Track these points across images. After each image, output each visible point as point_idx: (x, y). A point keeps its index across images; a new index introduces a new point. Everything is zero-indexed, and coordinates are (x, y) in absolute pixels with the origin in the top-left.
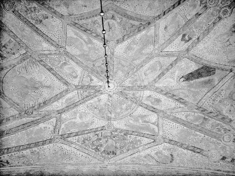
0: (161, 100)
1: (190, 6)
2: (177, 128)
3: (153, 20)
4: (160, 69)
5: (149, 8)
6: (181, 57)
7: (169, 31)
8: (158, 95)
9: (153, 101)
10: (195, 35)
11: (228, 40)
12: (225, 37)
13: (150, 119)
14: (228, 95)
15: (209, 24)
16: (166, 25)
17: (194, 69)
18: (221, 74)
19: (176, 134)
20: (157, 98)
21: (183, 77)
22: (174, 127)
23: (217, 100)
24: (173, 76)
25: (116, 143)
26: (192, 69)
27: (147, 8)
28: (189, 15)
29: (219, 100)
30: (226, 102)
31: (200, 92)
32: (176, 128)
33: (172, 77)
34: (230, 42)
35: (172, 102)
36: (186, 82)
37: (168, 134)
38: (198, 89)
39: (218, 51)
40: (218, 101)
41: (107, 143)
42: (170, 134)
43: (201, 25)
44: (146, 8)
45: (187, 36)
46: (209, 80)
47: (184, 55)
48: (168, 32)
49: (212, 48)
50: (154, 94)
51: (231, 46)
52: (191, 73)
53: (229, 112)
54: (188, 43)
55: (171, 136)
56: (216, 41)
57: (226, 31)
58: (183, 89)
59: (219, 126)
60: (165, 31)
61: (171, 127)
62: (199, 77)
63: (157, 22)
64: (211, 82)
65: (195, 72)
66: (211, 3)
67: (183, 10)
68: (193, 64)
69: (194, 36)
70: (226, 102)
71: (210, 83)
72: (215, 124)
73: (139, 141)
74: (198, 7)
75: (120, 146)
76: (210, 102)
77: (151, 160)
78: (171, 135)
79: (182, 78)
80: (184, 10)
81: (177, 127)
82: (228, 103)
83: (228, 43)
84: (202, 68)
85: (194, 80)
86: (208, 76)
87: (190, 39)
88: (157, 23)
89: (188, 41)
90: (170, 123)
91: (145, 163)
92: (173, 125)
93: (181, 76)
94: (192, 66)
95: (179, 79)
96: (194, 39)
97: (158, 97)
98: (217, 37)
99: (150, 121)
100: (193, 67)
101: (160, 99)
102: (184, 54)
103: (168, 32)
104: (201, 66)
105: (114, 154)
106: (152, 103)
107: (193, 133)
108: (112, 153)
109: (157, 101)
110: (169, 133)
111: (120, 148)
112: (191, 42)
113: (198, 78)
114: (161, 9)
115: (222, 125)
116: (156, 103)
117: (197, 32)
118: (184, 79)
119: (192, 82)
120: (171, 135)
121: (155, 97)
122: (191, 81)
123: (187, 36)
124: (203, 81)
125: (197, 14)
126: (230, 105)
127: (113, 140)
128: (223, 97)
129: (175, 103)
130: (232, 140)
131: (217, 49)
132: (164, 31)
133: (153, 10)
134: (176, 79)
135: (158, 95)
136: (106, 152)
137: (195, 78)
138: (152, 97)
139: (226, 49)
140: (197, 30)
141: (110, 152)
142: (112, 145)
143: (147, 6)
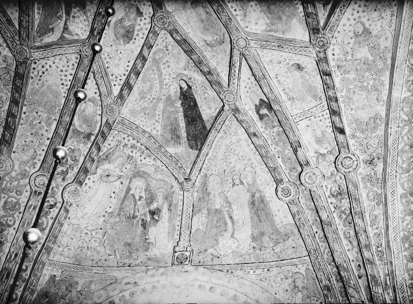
0: (131, 42)
1: (323, 133)
2: (63, 84)
3: (321, 44)
4: (206, 41)
5: (361, 30)
6: (225, 94)
7: (289, 74)
8: (144, 34)
9: (127, 23)
10: (266, 128)
11: (242, 183)
12: (249, 179)
13: (76, 20)
14: (143, 169)
15: (279, 157)
16: (306, 70)
17: (204, 112)
18: (187, 158)
19: (46, 83)
20: (136, 32)
21: (189, 87)
22: (63, 77)
23: (134, 151)
24: (190, 67)
26: (205, 108)
27: (363, 25)
28: (308, 126)
29: (133, 155)
30: (128, 168)
31: (154, 121)
32: (61, 82)
34: (238, 185)
36: (179, 93)
37: (43, 67)
38: (161, 117)
39: (229, 161)
40: (131, 154)
42: (44, 70)
43: (281, 144)
44: (364, 20)
45: (268, 113)
46: (178, 137)
47: (227, 102)
48: (286, 73)
49: (236, 153)
50: (145, 24)
51: (231, 185)
52: (196, 105)
53: (107, 174)
54: (254, 110)
55: (40, 73)
56: (246, 162)
57: (259, 182)
58: (161, 88)
59: (73, 162)
60: (292, 65)
61: (62, 71)
62: (188, 119)
63: (314, 52)
65: (198, 113)
66: (309, 174)
67: (323, 115)
68: (213, 111)
69: (264, 126)
71: (172, 138)
72: (77, 154)
74: (316, 146)
76: (129, 140)
78: (43, 73)
79: (188, 85)
80: (322, 118)
81: (65, 83)
82: (124, 169)
83: (237, 182)
84: (204, 127)
85: (181, 109)
86: (188, 134)
87: (261, 117)
88: (310, 51)
89: (258, 113)
90: (71, 66)
92: (67, 73)
93: (190, 84)
94: (210, 108)
95: (185, 78)
96: (259, 124)
97: (138, 35)
98: (253, 165)
99: (71, 19)
100: (208, 111)
101: (133, 40)
102: (230, 103)
103: (286, 73)
104: (208, 126)
106: (121, 21)
107: (53, 118)
109: (128, 32)
110: (47, 67)
112: (256, 117)
113: (186, 116)
114: (344, 63)
115: (75, 169)
116: (122, 31)
117: (272, 134)
118: (185, 89)
119: (179, 104)
120: (43, 73)
121: (137, 28)
122: (180, 102)
123: (268, 113)
124: (178, 126)
125: (300, 146)
126: (122, 174)
128: (139, 162)
129: (124, 75)
130: (39, 189)
131: (234, 159)
132: (292, 63)
133: (352, 41)
134: (186, 72)
135: (144, 34)
137: (185, 111)
138: (139, 19)
139: (229, 175)
140: (275, 134)
143: (367, 25)
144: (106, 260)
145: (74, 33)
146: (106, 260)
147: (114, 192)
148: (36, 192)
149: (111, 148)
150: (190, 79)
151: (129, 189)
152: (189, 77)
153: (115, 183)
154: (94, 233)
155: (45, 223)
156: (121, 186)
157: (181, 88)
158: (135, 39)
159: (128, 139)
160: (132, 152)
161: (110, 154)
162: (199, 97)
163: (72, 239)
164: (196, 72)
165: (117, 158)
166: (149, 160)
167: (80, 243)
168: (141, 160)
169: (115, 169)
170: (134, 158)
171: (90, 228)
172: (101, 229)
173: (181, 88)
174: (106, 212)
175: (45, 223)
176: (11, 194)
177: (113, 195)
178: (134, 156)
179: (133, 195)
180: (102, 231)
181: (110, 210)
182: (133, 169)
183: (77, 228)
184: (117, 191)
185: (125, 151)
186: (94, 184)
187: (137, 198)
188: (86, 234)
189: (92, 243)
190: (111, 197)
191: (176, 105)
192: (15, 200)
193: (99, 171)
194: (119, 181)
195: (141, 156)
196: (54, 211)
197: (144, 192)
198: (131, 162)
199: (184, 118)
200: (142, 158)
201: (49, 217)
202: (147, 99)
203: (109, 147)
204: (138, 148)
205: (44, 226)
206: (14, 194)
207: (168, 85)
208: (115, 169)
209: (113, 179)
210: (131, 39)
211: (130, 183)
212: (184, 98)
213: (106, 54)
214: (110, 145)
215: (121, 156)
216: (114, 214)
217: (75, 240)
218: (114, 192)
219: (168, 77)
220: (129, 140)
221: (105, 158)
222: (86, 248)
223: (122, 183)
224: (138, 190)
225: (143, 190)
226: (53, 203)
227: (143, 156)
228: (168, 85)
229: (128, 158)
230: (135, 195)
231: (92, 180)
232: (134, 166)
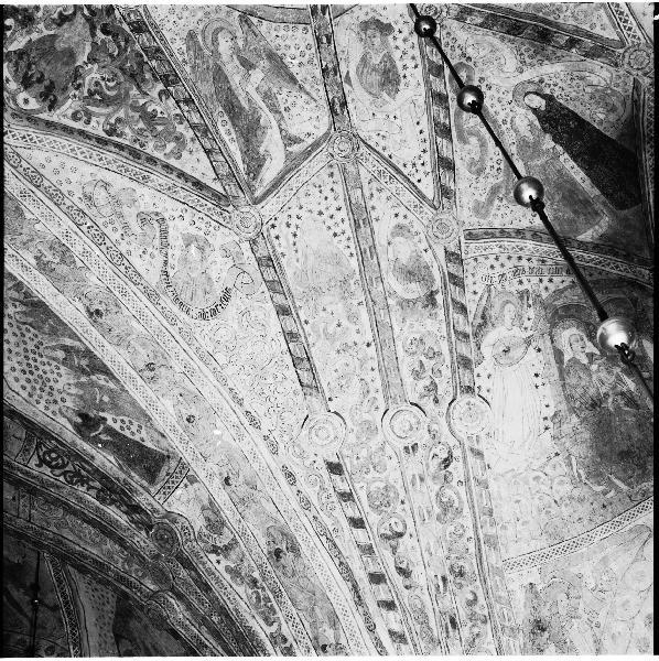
0: (401, 87)
2: (335, 235)
6: (626, 60)
8: (413, 58)
9: (376, 60)
13: (294, 111)
19: (309, 251)
20: (399, 65)
21: (549, 99)
22: (330, 222)
23: (524, 279)
25: (92, 59)
29: (526, 286)
30: (532, 316)
32: (331, 233)
33: (524, 62)
35: (422, 136)
37: (288, 225)
40: (521, 288)
41: (59, 25)
42: (293, 229)
46: (586, 203)
47: (640, 73)
53: (501, 349)
55: (292, 239)
59: (433, 362)
61: (321, 213)
64: (582, 217)
70: (532, 316)
71: (575, 212)
72: (429, 342)
73: (177, 139)
75: (97, 84)
76: (502, 265)
77: (150, 250)
78: (295, 235)
79: (544, 96)
81: (338, 231)
82: (528, 324)
85: (559, 148)
90: (331, 196)
91: (123, 248)
92: (332, 211)
95: (531, 88)
97: (405, 67)
101: (403, 80)
105: (48, 103)
106: (364, 60)
107: (355, 303)
108: (40, 88)
109: (386, 72)
110: (294, 221)
111: (91, 94)
115: (443, 369)
116: (376, 78)
118: (543, 108)
119: (548, 143)
120: (295, 235)
121: (397, 55)
124: (573, 183)
126: (530, 333)
127: (93, 35)
129: (424, 151)
130: (409, 440)
134: (526, 76)
135: (413, 58)
136: (23, 64)
137: (567, 149)
138: (390, 38)
141: (40, 81)
142: (71, 55)
144: (604, 506)
145: (302, 137)
146: (604, 506)
147: (536, 375)
148: (406, 448)
150: (541, 81)
151: (559, 354)
152: (537, 80)
154: (548, 470)
155: (455, 497)
157: (535, 111)
158: (405, 77)
159: (499, 263)
160: (521, 282)
161: (485, 309)
162: (578, 104)
163: (518, 501)
164: (546, 62)
166: (560, 279)
167: (537, 502)
168: (546, 288)
171: (536, 465)
172: (557, 454)
173: (535, 111)
174: (546, 418)
175: (455, 497)
176: (369, 476)
177: (539, 381)
179: (574, 361)
180: (560, 457)
181: (550, 412)
183: (514, 477)
184: (539, 369)
185: (507, 288)
187: (585, 361)
188: (536, 478)
189: (558, 492)
190: (537, 387)
191: (544, 148)
192: (382, 485)
193: (486, 350)
194: (531, 348)
195: (541, 281)
196: (455, 468)
197: (589, 344)
198: (531, 302)
199: (575, 161)
200: (545, 282)
201: (454, 483)
202: (487, 171)
203: (477, 298)
204: (527, 269)
205: (456, 505)
206: (373, 473)
207: (509, 120)
210: (398, 84)
211: (552, 342)
212: (551, 125)
213: (374, 135)
214: (475, 293)
215: (507, 302)
216: (562, 413)
217: (523, 501)
218: (536, 375)
219: (498, 107)
220: (502, 265)
221: (481, 321)
222: (553, 504)
223: (539, 350)
224: (577, 346)
225: (585, 339)
226: (446, 456)
227: (546, 279)
228: (509, 120)
229: (521, 298)
230: (578, 357)
231: (484, 375)
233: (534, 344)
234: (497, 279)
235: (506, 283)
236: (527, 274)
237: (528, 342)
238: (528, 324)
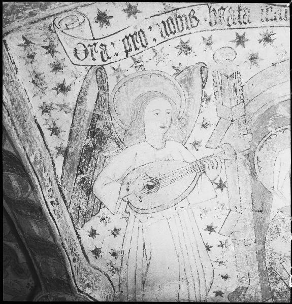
29: (201, 53)
30: (212, 118)
40: (187, 61)
53: (142, 182)
70: (212, 118)
82: (202, 135)
126: (203, 152)
128: (247, 72)
147: (210, 229)
149: (80, 100)
153: (193, 198)
156: (223, 196)
160: (185, 48)
161: (95, 118)
165: (137, 113)
168: (253, 58)
169: (160, 154)
170: (212, 67)
177: (213, 239)
178: (208, 61)
182: (239, 110)
185: (150, 66)
186: (119, 238)
190: (208, 248)
194: (204, 182)
195: (240, 40)
198: (210, 90)
203: (71, 98)
208: (160, 154)
209: (180, 187)
214: (63, 88)
218: (210, 229)
223: (221, 186)
232: (230, 100)
233: (211, 173)
234: (120, 48)
235: (147, 54)
236: (204, 25)
237: (200, 169)
238: (202, 135)
